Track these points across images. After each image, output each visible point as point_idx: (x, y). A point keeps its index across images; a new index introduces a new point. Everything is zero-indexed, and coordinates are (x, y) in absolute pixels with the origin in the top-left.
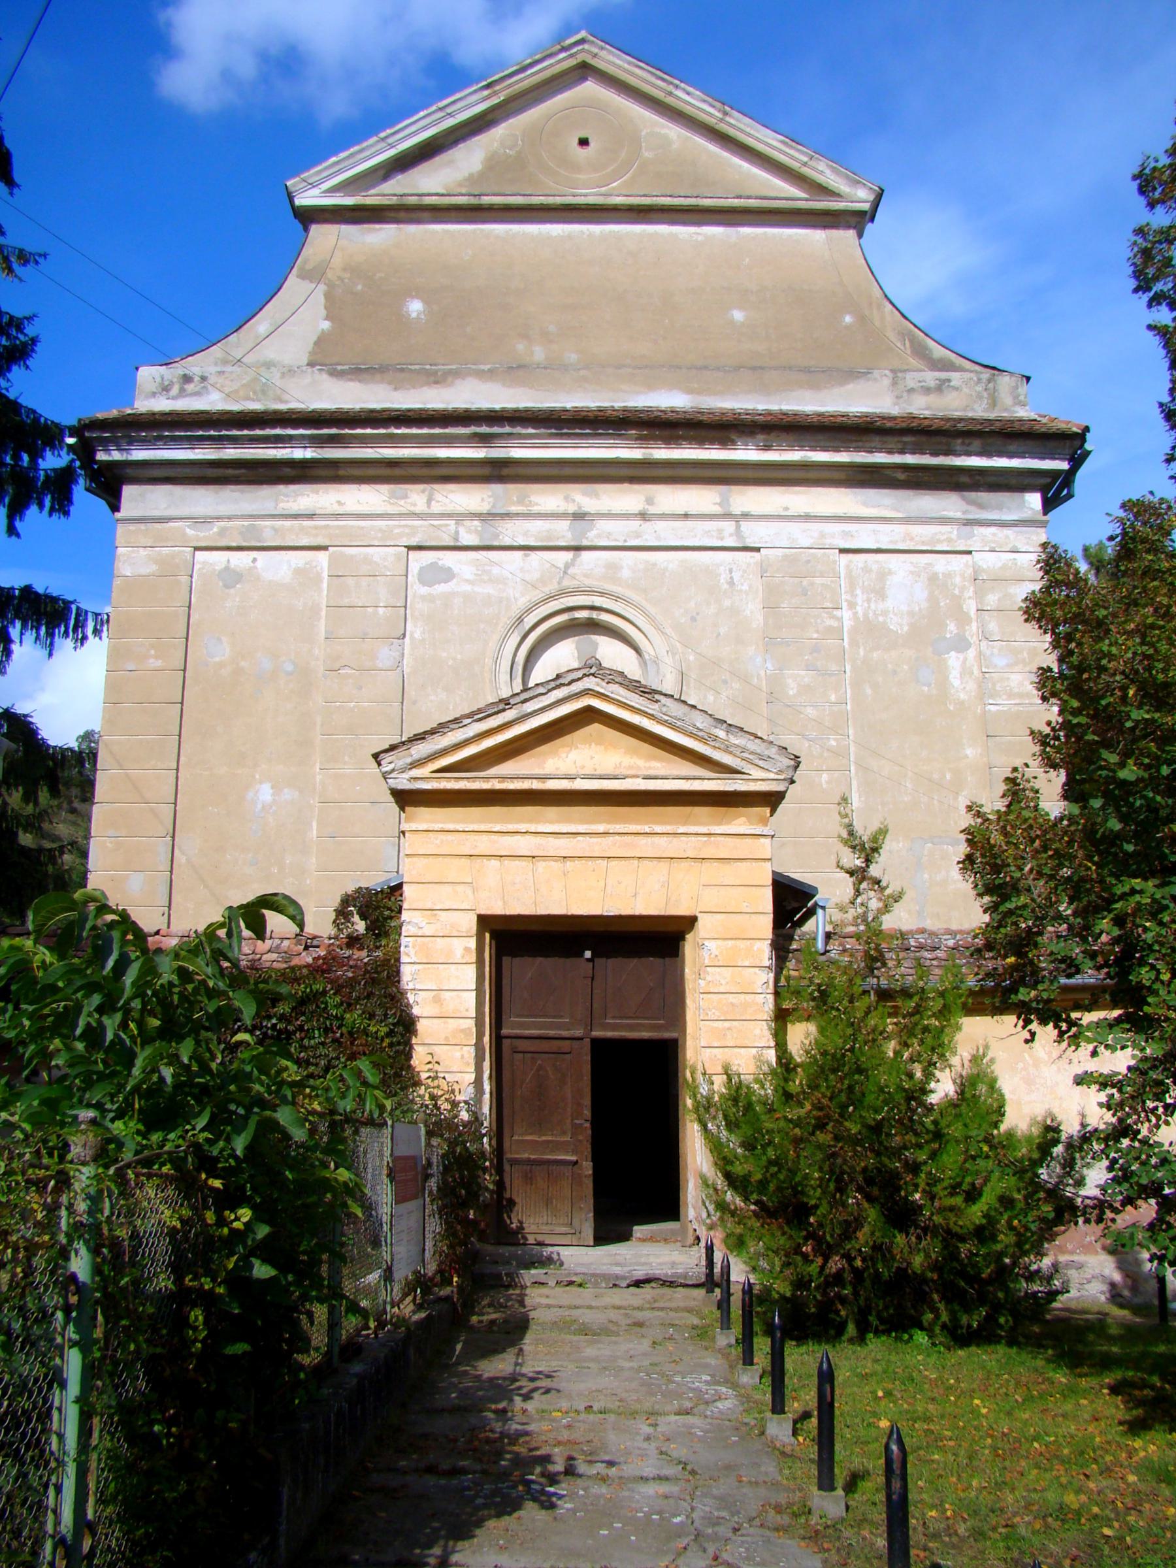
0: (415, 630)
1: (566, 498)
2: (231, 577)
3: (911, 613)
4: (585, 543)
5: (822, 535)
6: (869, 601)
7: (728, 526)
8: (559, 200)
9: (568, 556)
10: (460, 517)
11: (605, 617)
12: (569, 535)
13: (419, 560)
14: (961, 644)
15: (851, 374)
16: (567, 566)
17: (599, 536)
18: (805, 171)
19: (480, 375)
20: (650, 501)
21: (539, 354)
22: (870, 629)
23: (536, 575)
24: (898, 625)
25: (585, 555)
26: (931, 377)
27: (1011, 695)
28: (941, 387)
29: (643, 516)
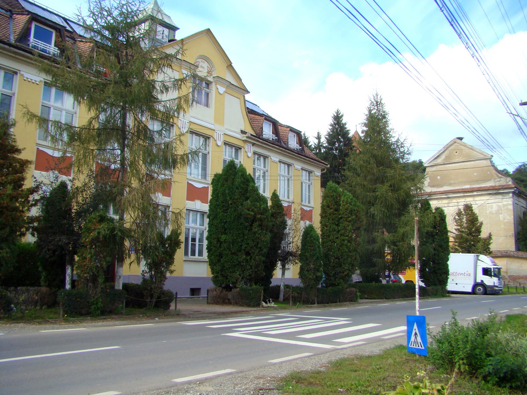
14: (501, 214)
21: (453, 182)
22: (491, 213)
28: (500, 181)
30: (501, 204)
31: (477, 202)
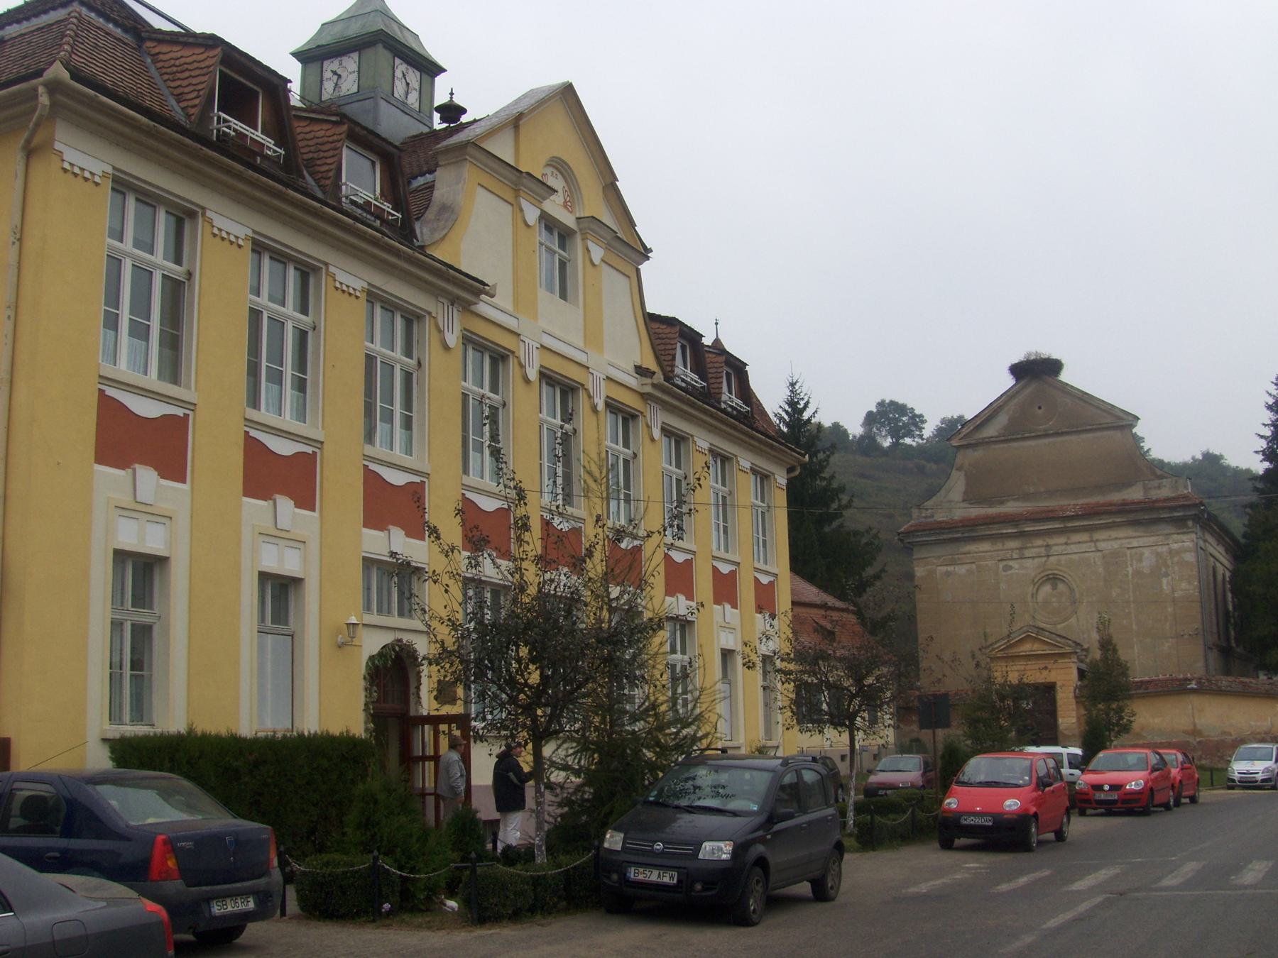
0: (1003, 586)
2: (948, 574)
10: (1012, 550)
13: (1001, 565)
14: (1166, 575)
15: (1129, 485)
21: (1032, 490)
22: (1138, 573)
24: (1146, 571)
26: (1156, 483)
29: (1066, 544)
30: (1165, 549)
31: (1102, 545)
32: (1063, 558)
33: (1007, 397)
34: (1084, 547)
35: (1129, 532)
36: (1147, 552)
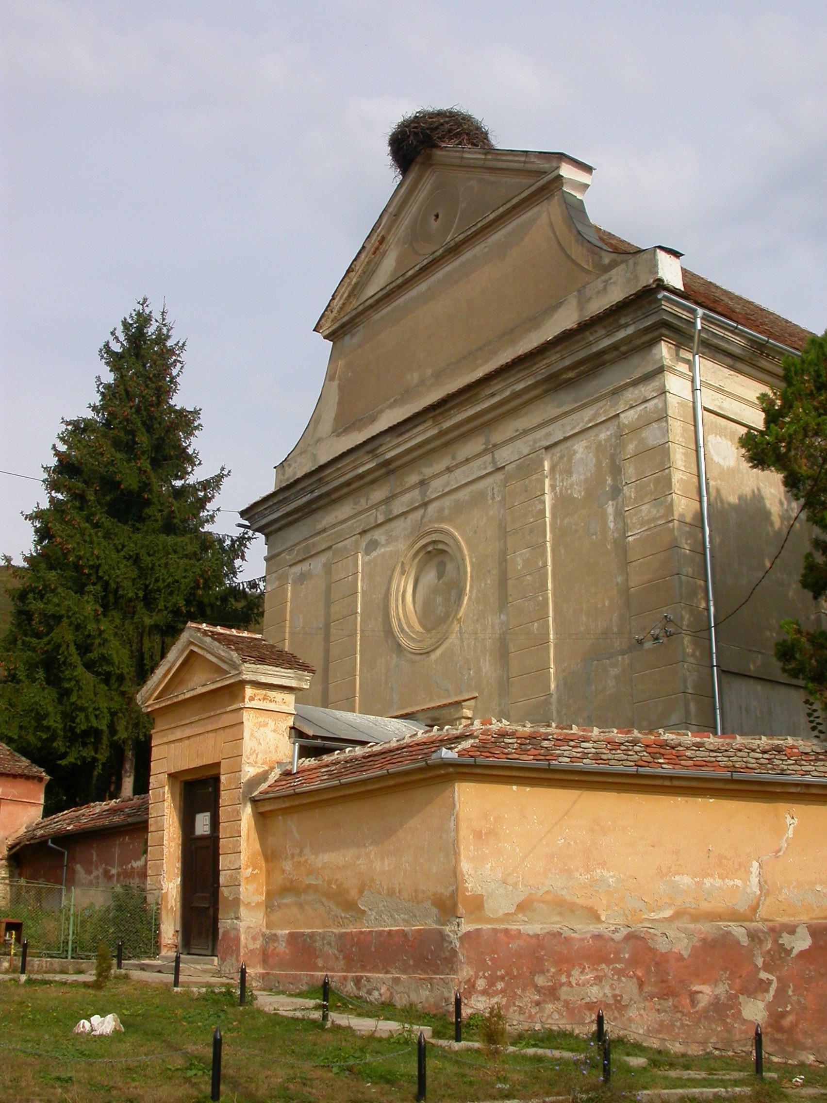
1: (420, 473)
3: (586, 479)
4: (427, 499)
5: (535, 442)
6: (562, 481)
7: (488, 458)
8: (417, 268)
9: (421, 512)
11: (440, 546)
12: (419, 498)
16: (423, 517)
17: (432, 492)
18: (528, 166)
19: (390, 407)
20: (454, 458)
21: (415, 377)
23: (409, 530)
25: (432, 508)
26: (599, 284)
27: (642, 524)
29: (449, 470)
32: (447, 502)
33: (393, 212)
34: (476, 469)
35: (549, 409)
36: (580, 447)
